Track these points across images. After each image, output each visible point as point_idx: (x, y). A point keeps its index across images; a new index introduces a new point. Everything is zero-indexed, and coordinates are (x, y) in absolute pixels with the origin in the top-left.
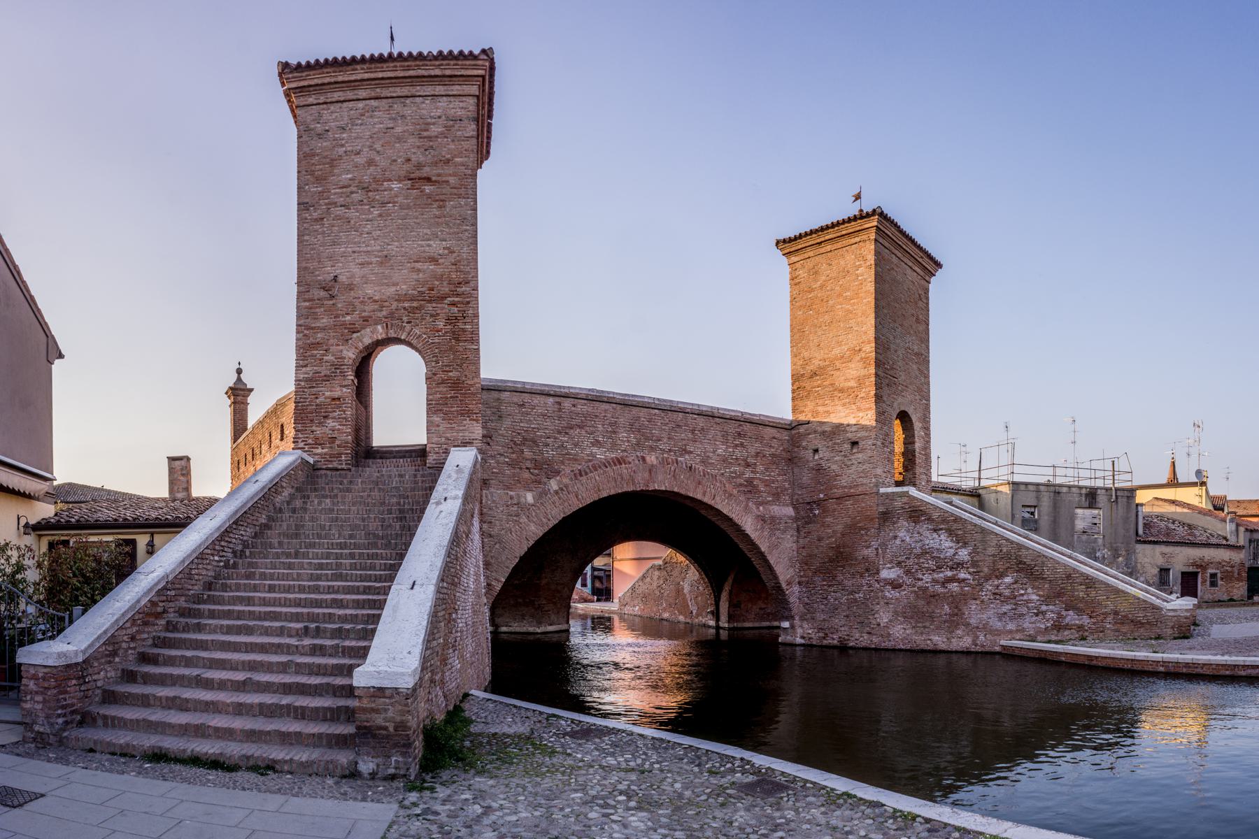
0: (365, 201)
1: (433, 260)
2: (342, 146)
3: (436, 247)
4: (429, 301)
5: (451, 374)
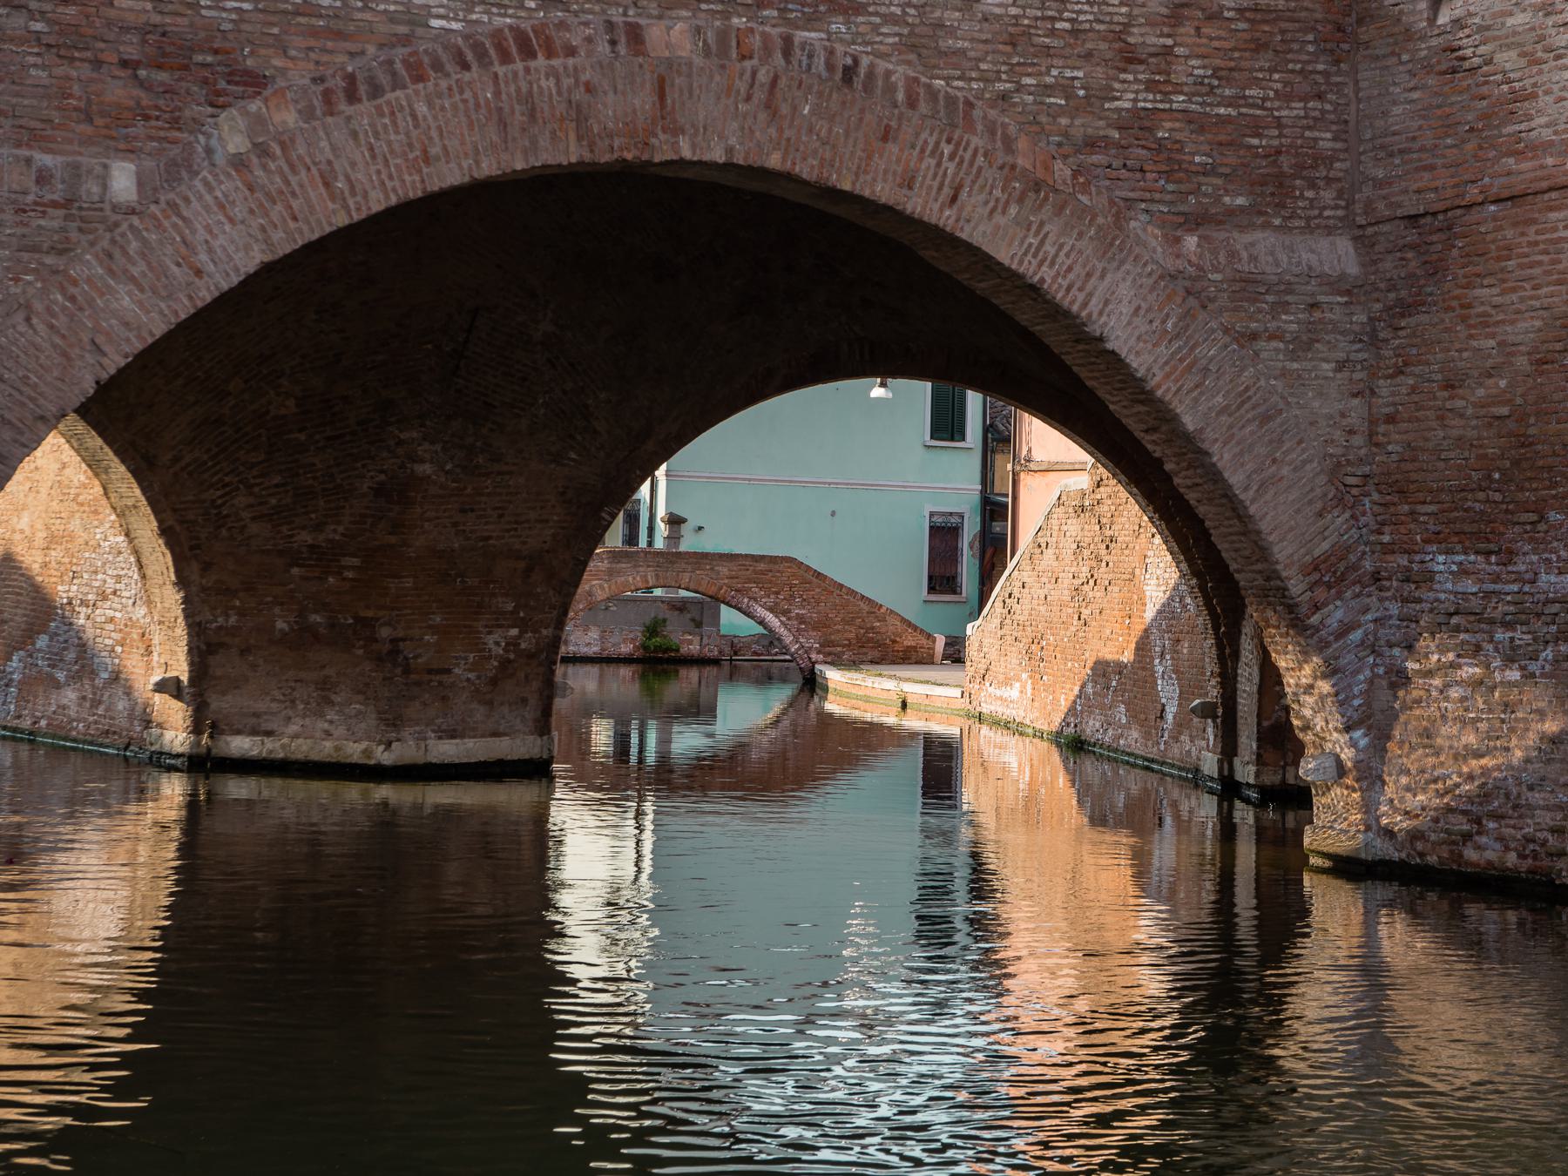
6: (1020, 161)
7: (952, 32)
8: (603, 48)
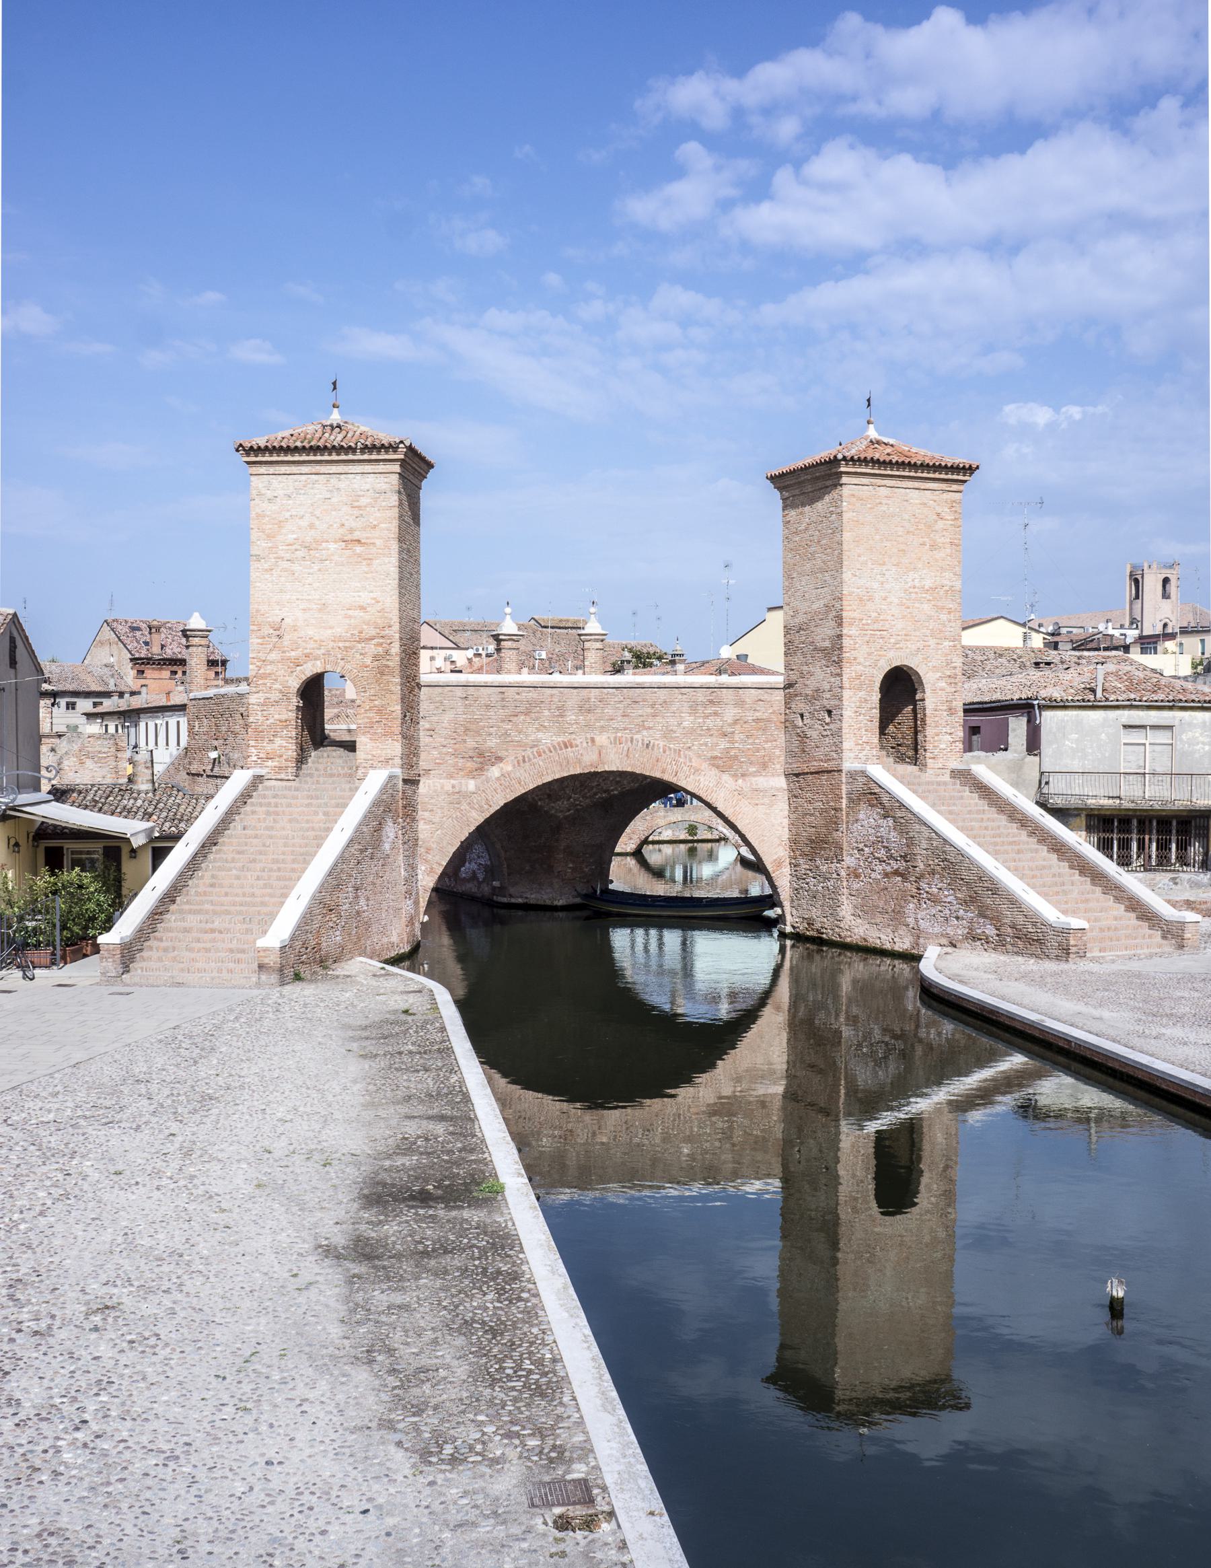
0: (307, 558)
1: (362, 608)
2: (288, 511)
3: (365, 598)
4: (359, 642)
5: (376, 702)
6: (694, 764)
7: (675, 732)
8: (585, 744)
